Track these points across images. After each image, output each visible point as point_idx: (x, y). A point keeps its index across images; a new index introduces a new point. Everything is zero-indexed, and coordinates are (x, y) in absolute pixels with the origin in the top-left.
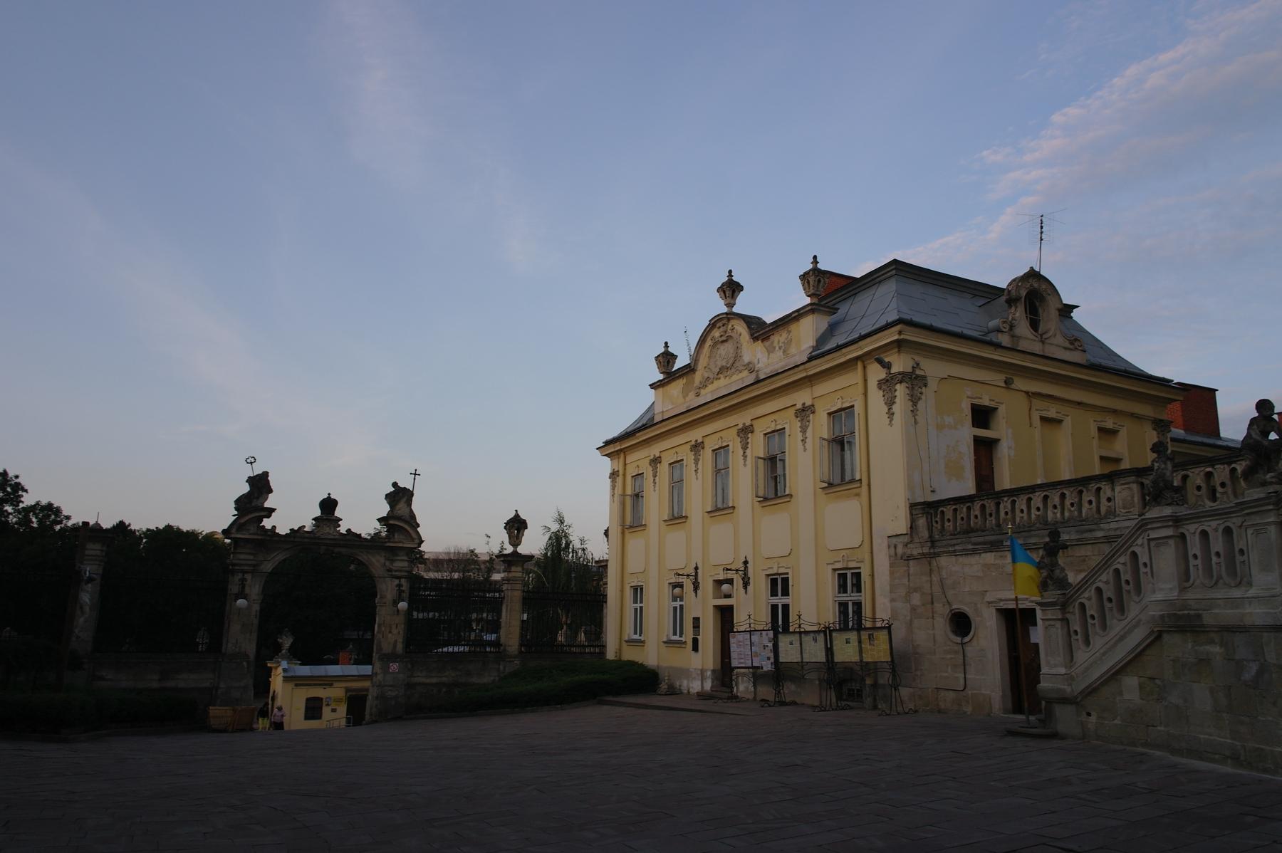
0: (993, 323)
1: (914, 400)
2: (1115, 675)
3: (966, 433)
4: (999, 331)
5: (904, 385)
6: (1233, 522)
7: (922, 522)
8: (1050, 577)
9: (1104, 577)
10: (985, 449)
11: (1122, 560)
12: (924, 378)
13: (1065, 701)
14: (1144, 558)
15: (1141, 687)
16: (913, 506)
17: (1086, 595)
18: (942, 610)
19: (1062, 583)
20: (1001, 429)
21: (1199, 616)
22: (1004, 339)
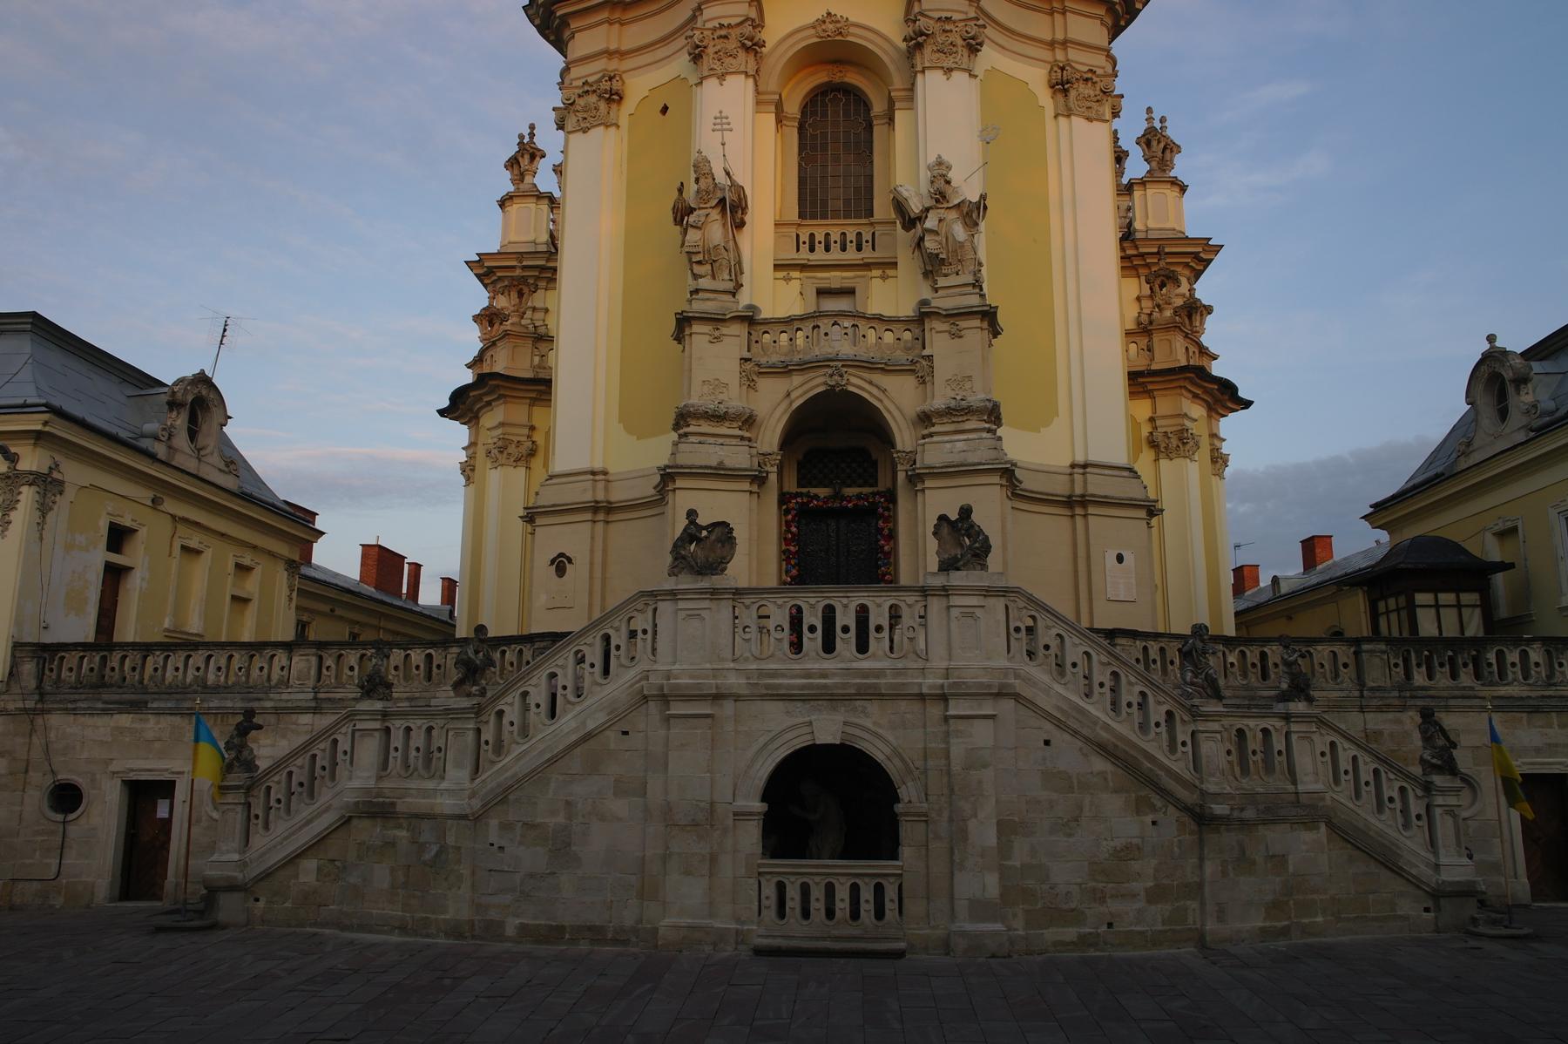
0: (150, 427)
1: (44, 509)
2: (294, 859)
3: (100, 555)
4: (156, 438)
5: (34, 489)
6: (438, 723)
7: (28, 668)
8: (237, 758)
9: (299, 762)
10: (115, 575)
11: (322, 746)
12: (61, 483)
13: (233, 887)
14: (344, 744)
15: (319, 869)
16: (17, 646)
17: (276, 778)
18: (40, 782)
19: (250, 766)
20: (136, 556)
21: (393, 804)
22: (160, 450)
